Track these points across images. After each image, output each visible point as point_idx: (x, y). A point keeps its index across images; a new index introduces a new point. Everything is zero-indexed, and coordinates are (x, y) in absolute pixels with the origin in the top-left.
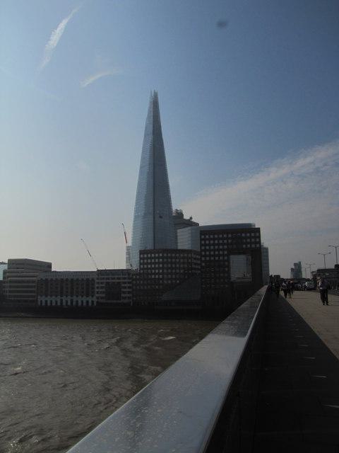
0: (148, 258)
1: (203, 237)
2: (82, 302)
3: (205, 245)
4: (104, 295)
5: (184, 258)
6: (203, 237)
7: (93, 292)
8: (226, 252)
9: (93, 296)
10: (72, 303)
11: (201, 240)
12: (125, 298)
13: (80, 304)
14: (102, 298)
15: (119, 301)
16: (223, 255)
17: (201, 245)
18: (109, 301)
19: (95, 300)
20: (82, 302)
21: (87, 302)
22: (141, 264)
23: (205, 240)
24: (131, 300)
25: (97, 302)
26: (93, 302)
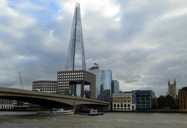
0: (35, 85)
1: (59, 75)
2: (7, 107)
3: (60, 79)
4: (16, 103)
5: (53, 85)
6: (59, 75)
7: (12, 102)
8: (68, 82)
9: (12, 104)
10: (2, 107)
11: (58, 76)
12: (25, 105)
13: (6, 108)
14: (16, 105)
15: (22, 106)
16: (67, 84)
17: (58, 79)
18: (19, 106)
19: (13, 106)
20: (7, 107)
21: (10, 107)
22: (33, 88)
23: (60, 76)
24: (28, 106)
25: (14, 108)
26: (12, 107)
